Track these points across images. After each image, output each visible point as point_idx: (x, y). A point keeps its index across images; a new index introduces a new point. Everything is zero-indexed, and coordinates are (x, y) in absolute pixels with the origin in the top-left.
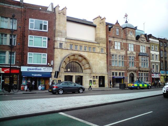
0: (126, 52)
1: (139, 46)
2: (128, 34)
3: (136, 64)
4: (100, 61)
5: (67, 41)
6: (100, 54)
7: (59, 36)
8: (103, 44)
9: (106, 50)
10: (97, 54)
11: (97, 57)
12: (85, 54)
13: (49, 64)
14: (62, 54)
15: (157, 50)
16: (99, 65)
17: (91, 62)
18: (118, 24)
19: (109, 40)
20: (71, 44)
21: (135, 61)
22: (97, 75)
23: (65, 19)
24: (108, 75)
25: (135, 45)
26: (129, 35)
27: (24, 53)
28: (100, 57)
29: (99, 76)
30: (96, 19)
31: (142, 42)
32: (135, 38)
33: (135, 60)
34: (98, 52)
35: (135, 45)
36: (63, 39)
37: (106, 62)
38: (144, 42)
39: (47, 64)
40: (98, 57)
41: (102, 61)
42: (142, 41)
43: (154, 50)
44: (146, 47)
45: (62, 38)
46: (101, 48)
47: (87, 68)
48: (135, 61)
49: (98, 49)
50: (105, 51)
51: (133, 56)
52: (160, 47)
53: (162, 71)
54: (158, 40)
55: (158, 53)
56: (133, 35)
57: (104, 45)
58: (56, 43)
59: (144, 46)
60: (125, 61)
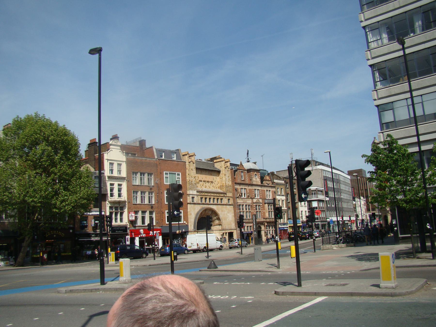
0: (252, 201)
1: (265, 190)
2: (253, 177)
3: (262, 215)
4: (228, 214)
6: (227, 206)
11: (225, 209)
12: (214, 207)
13: (185, 222)
14: (195, 209)
15: (283, 194)
16: (227, 219)
17: (221, 216)
18: (242, 166)
20: (202, 196)
21: (261, 211)
22: (226, 231)
24: (237, 231)
25: (261, 190)
26: (254, 179)
27: (162, 211)
28: (228, 209)
30: (219, 163)
31: (267, 186)
32: (260, 181)
33: (262, 209)
35: (261, 191)
36: (195, 192)
37: (233, 214)
38: (269, 185)
39: (184, 222)
40: (226, 209)
42: (267, 185)
43: (279, 194)
44: (272, 191)
47: (216, 224)
48: (261, 211)
49: (225, 199)
50: (231, 202)
51: (259, 204)
52: (286, 190)
53: (289, 221)
54: (283, 180)
55: (284, 198)
56: (258, 178)
59: (270, 191)
60: (251, 211)
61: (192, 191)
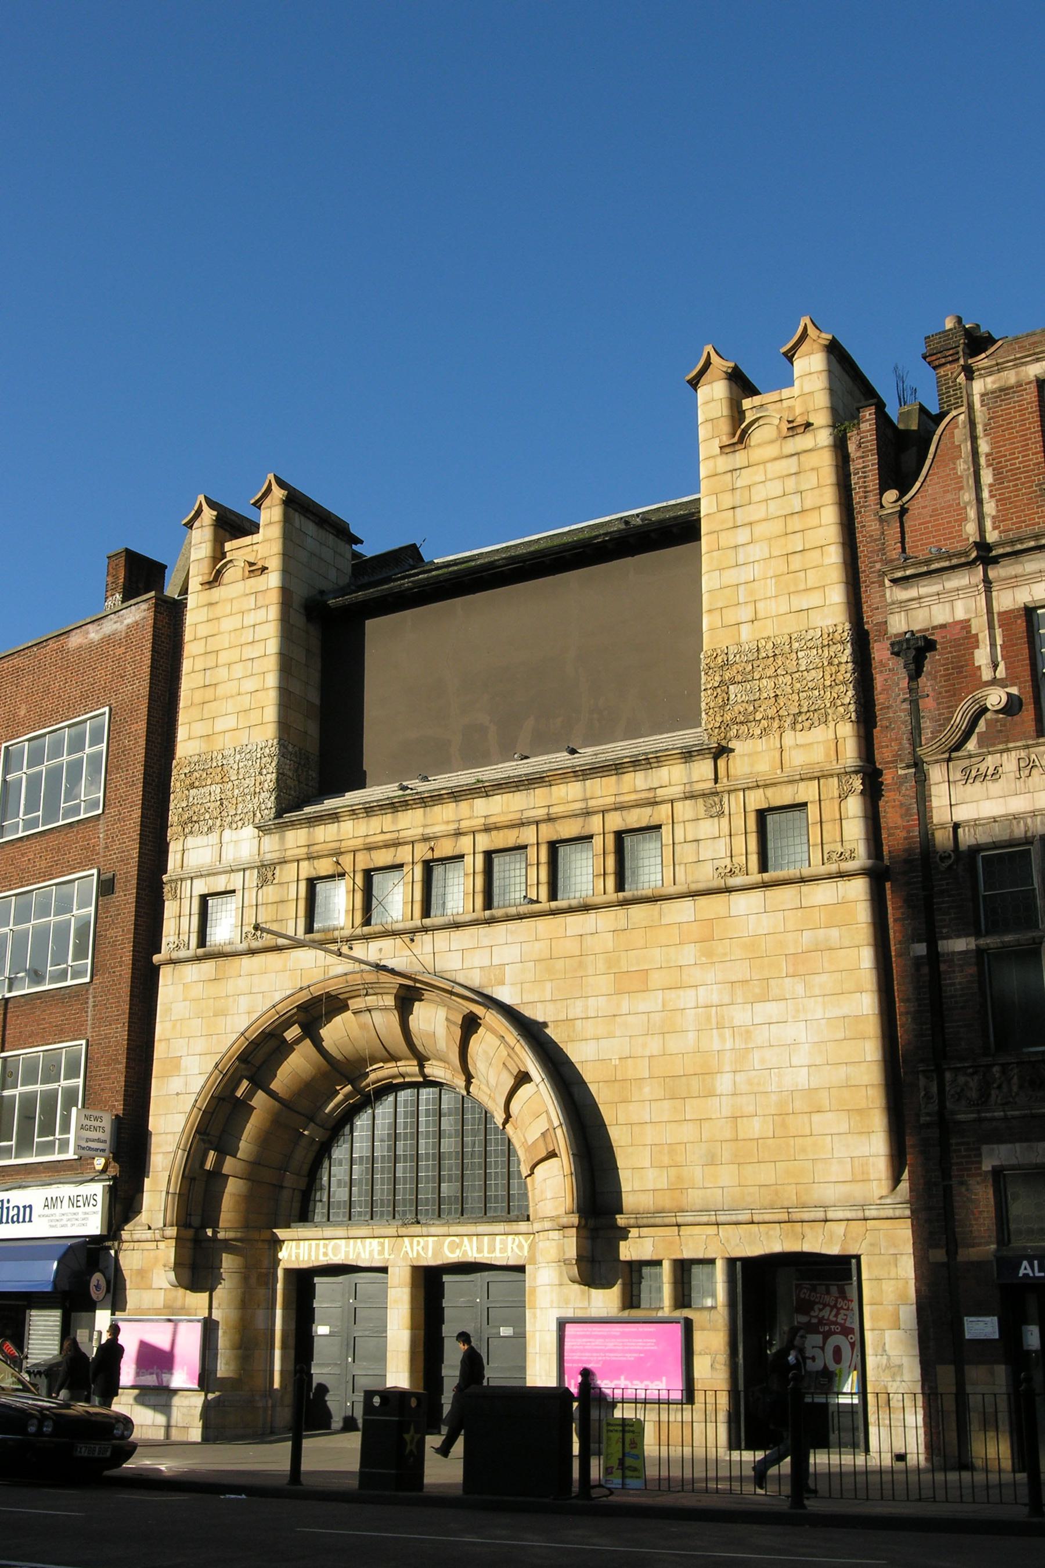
4: (741, 1015)
5: (271, 844)
6: (742, 903)
7: (189, 823)
8: (789, 737)
9: (854, 805)
10: (683, 911)
11: (689, 954)
16: (724, 1083)
19: (898, 624)
23: (260, 615)
29: (731, 1262)
34: (720, 883)
41: (772, 1010)
45: (227, 833)
46: (757, 800)
57: (821, 734)
58: (170, 909)
61: (213, 838)
